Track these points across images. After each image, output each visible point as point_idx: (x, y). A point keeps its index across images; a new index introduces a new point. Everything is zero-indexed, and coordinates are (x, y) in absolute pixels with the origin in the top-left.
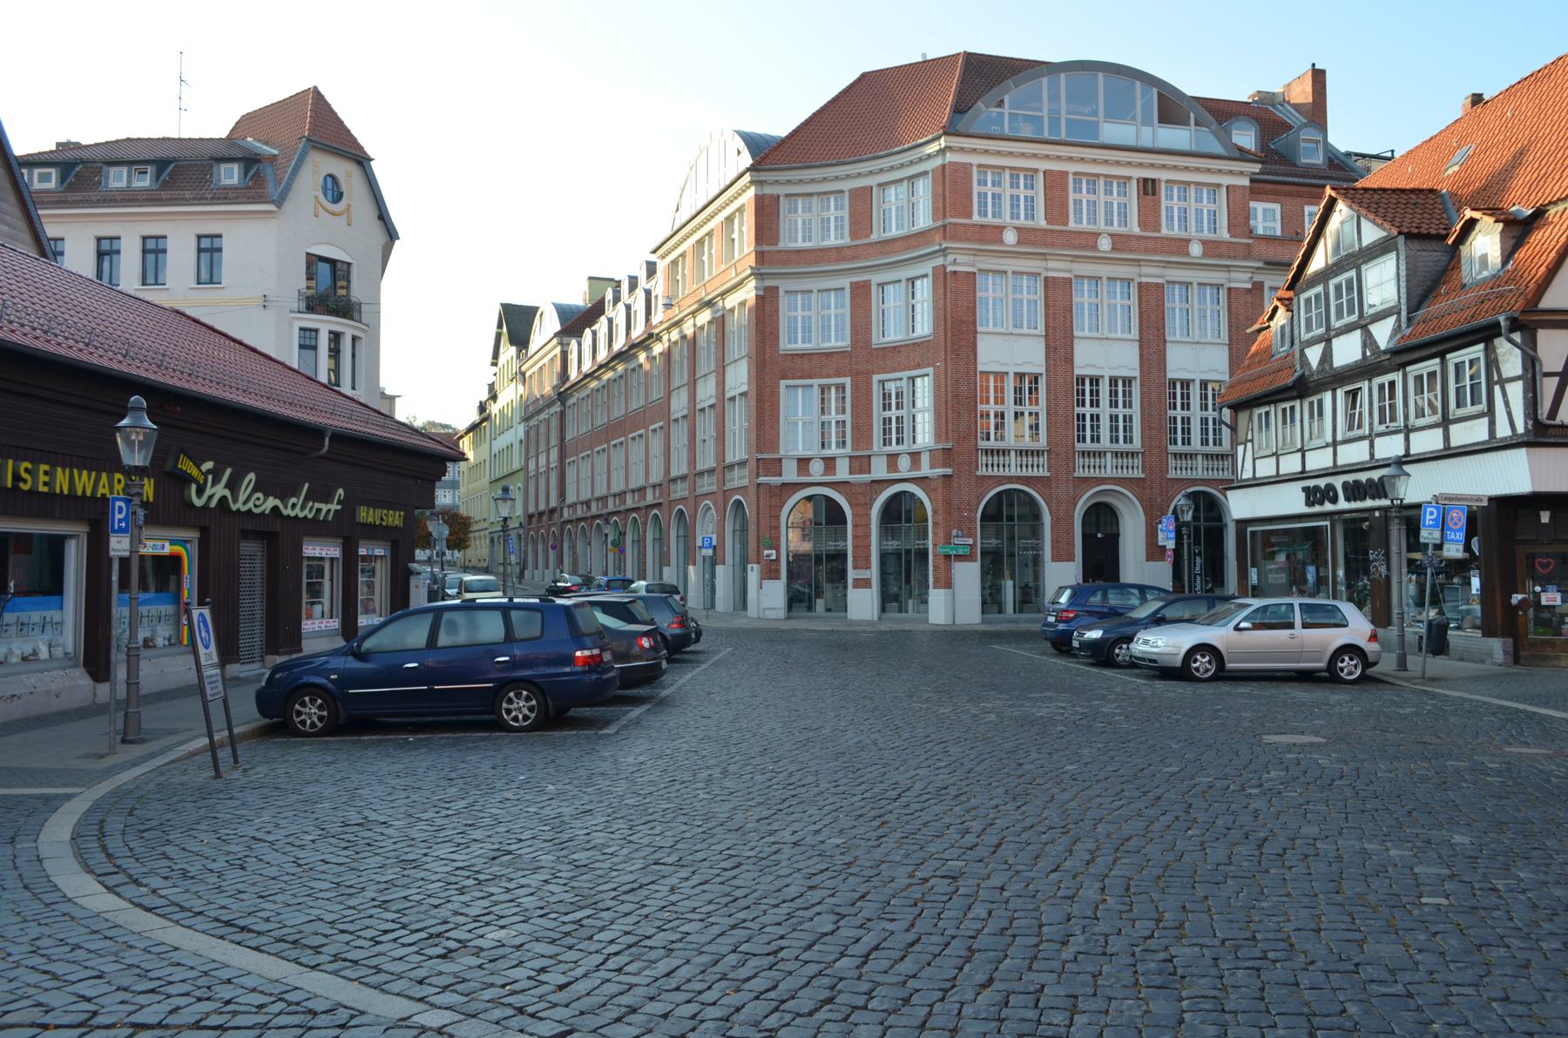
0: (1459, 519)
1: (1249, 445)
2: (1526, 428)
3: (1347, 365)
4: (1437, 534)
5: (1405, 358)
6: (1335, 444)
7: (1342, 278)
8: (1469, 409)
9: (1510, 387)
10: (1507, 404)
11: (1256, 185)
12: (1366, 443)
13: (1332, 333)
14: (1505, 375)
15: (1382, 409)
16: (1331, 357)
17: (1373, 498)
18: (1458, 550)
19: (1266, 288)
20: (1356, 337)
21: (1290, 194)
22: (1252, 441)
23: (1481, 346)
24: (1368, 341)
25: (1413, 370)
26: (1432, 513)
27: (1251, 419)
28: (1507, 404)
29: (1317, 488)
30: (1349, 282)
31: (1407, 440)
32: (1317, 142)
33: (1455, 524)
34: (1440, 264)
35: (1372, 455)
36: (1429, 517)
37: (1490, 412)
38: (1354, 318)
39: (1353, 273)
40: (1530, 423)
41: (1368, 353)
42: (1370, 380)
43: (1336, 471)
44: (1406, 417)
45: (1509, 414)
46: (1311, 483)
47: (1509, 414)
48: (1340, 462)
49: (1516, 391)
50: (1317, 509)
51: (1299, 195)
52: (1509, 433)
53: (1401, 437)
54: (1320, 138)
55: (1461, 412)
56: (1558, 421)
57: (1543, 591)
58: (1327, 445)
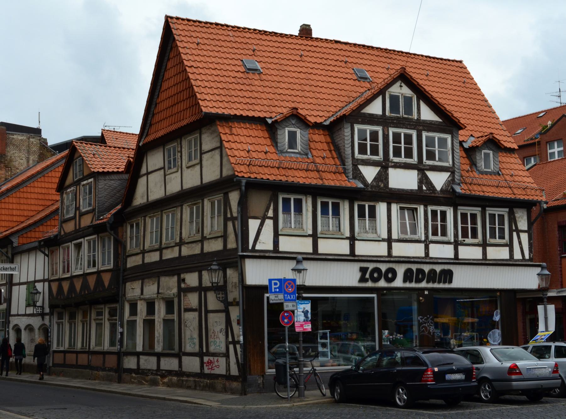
2: (530, 257)
3: (403, 190)
10: (520, 243)
23: (507, 210)
24: (424, 180)
25: (462, 209)
28: (520, 243)
35: (427, 254)
37: (510, 246)
41: (424, 188)
44: (456, 235)
52: (521, 258)
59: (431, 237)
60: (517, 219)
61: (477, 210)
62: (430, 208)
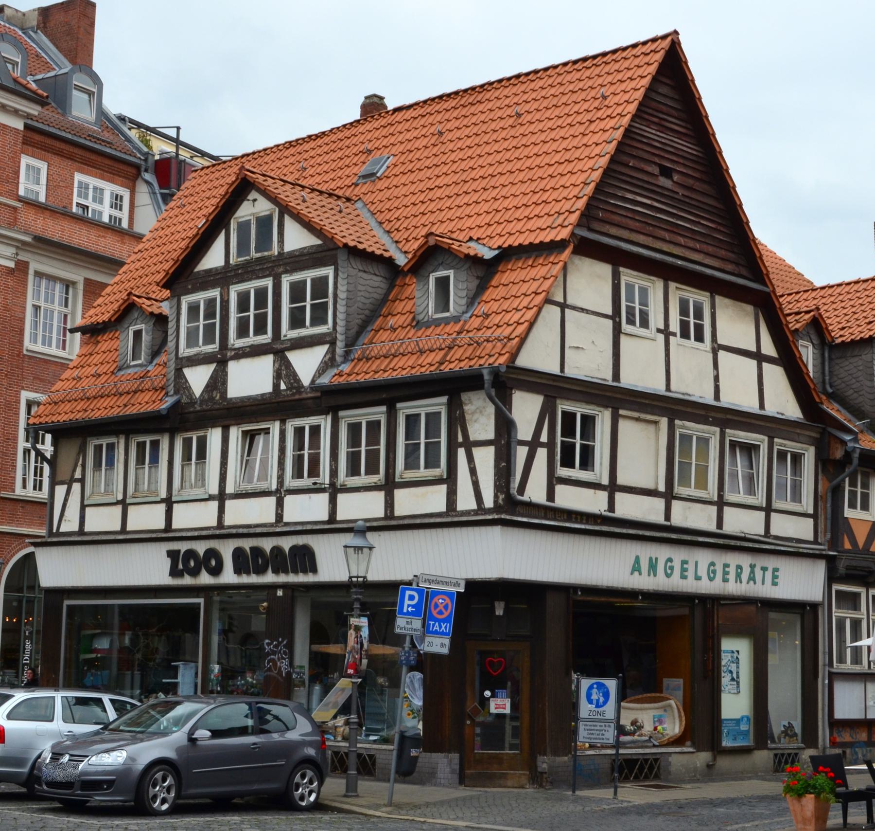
0: (446, 607)
1: (76, 487)
3: (249, 398)
4: (417, 624)
5: (342, 401)
6: (222, 497)
7: (251, 286)
8: (423, 473)
9: (477, 452)
10: (473, 471)
11: (30, 134)
12: (272, 501)
13: (229, 354)
14: (473, 437)
15: (298, 461)
16: (225, 383)
17: (276, 571)
18: (442, 645)
19: (31, 272)
20: (266, 363)
21: (60, 154)
22: (82, 481)
23: (444, 399)
24: (284, 370)
25: (348, 416)
26: (411, 598)
27: (83, 451)
28: (473, 471)
29: (190, 553)
30: (261, 294)
31: (333, 502)
32: (90, 93)
33: (440, 613)
34: (379, 291)
35: (279, 517)
36: (409, 601)
37: (450, 480)
38: (266, 338)
39: (268, 282)
40: (501, 497)
41: (283, 386)
42: (283, 422)
43: (222, 533)
44: (334, 473)
45: (476, 484)
46: (183, 547)
47: (476, 484)
48: (228, 521)
49: (485, 458)
50: (187, 580)
51: (71, 158)
52: (473, 506)
53: (324, 497)
54: (95, 90)
55: (410, 475)
56: (525, 498)
57: (493, 696)
58: (211, 498)
59: (290, 482)
60: (467, 417)
61: (379, 413)
62: (291, 425)
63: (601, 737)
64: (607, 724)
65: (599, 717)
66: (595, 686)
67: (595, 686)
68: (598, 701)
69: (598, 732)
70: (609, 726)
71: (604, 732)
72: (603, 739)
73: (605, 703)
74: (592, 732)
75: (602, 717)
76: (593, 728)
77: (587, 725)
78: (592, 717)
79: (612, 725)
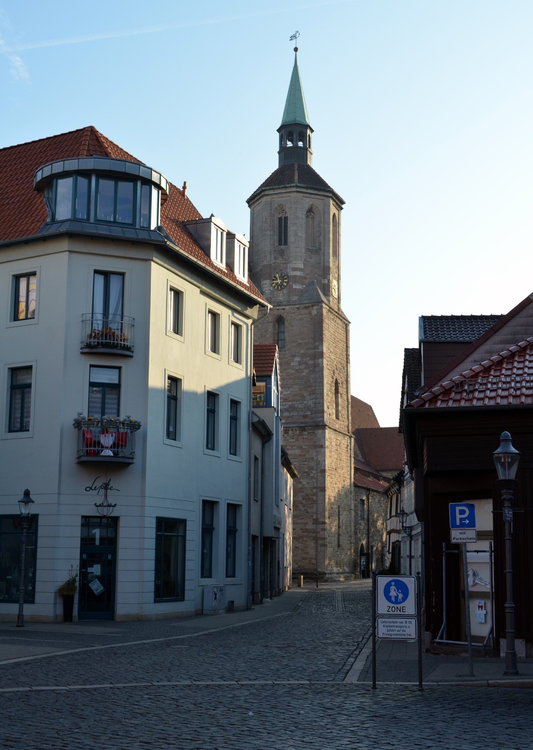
63: (402, 633)
64: (408, 620)
65: (399, 613)
66: (393, 583)
67: (393, 583)
68: (396, 597)
69: (399, 629)
70: (411, 622)
71: (404, 629)
72: (405, 635)
73: (404, 599)
74: (392, 628)
75: (402, 613)
76: (392, 624)
77: (386, 622)
78: (392, 613)
79: (413, 621)
